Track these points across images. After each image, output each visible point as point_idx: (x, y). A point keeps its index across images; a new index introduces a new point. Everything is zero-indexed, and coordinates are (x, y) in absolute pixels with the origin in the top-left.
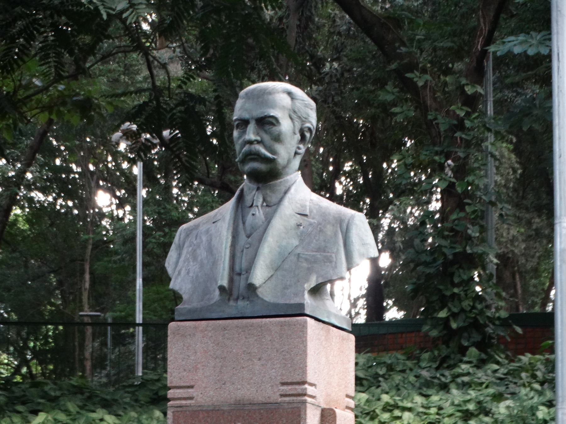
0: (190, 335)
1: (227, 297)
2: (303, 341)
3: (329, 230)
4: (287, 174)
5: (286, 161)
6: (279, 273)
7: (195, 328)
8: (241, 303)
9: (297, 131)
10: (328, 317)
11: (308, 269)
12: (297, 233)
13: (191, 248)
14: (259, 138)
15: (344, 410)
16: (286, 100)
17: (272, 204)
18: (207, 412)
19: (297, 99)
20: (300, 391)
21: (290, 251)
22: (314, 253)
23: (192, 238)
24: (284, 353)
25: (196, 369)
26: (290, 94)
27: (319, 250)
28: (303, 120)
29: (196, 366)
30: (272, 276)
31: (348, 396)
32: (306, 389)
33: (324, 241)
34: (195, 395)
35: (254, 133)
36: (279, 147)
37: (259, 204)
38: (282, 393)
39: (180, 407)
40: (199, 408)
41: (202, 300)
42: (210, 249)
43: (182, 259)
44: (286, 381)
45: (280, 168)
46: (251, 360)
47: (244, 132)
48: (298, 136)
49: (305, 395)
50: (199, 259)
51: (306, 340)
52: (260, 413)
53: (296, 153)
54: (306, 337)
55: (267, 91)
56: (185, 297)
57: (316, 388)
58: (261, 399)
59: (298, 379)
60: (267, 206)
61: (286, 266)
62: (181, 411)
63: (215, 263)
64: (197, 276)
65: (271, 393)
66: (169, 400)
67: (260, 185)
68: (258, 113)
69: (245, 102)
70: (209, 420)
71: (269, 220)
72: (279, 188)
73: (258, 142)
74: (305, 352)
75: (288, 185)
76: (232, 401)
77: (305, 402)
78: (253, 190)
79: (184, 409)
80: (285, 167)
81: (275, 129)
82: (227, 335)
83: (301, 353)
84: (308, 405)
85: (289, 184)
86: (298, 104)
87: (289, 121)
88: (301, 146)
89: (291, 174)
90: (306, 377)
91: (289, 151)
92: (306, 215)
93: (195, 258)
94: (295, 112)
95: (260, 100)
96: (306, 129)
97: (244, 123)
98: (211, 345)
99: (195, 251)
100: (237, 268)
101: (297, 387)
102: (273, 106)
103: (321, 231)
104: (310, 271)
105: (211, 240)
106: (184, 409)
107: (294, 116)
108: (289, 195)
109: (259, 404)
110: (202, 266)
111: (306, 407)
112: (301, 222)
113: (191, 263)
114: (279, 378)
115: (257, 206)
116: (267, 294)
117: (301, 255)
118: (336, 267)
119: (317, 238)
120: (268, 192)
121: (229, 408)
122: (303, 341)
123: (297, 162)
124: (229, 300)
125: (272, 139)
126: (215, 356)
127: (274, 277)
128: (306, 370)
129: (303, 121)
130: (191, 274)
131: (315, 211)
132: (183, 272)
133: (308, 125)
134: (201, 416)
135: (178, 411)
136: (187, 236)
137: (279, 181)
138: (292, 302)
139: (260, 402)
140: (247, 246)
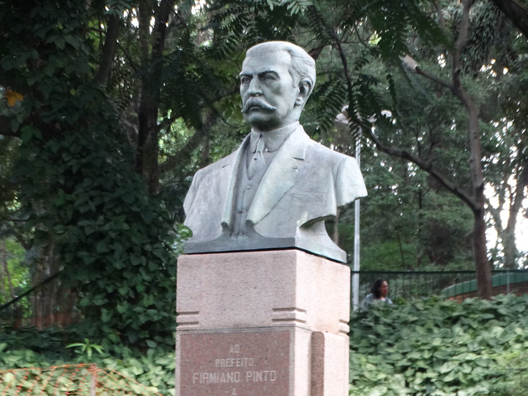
0: (196, 267)
1: (229, 233)
2: (292, 271)
3: (322, 172)
4: (288, 123)
6: (275, 211)
7: (201, 260)
8: (240, 238)
9: (296, 85)
10: (320, 250)
11: (301, 207)
13: (203, 190)
14: (260, 91)
15: (337, 334)
16: (286, 58)
17: (273, 150)
18: (210, 334)
19: (296, 56)
20: (289, 316)
22: (307, 193)
23: (205, 181)
24: (276, 282)
25: (201, 296)
26: (290, 51)
27: (311, 190)
28: (302, 75)
29: (201, 294)
30: (268, 213)
31: (341, 321)
32: (294, 314)
33: (317, 182)
34: (199, 320)
35: (256, 87)
36: (278, 99)
37: (261, 150)
38: (274, 318)
39: (187, 330)
40: (204, 332)
41: (208, 236)
42: (218, 191)
43: (196, 199)
44: (278, 307)
45: (280, 117)
46: (249, 289)
47: (247, 87)
48: (298, 89)
49: (294, 319)
50: (209, 199)
51: (295, 271)
52: (255, 336)
53: (296, 105)
54: (295, 268)
55: (269, 49)
56: (195, 233)
57: (306, 313)
58: (256, 323)
59: (287, 305)
60: (268, 151)
61: (282, 204)
62: (188, 335)
63: (220, 203)
64: (206, 215)
65: (265, 318)
66: (177, 325)
67: (263, 133)
68: (260, 69)
69: (250, 59)
70: (211, 342)
71: (268, 163)
73: (260, 95)
74: (294, 281)
75: (287, 133)
76: (231, 325)
77: (293, 326)
78: (257, 137)
79: (191, 332)
80: (284, 117)
81: (275, 83)
82: (227, 266)
83: (291, 282)
84: (296, 329)
85: (289, 132)
86: (297, 60)
87: (289, 76)
88: (301, 98)
89: (291, 123)
90: (295, 303)
91: (290, 103)
92: (302, 160)
93: (205, 198)
94: (294, 67)
95: (263, 57)
96: (306, 83)
97: (249, 77)
98: (215, 275)
99: (206, 192)
100: (239, 207)
101: (287, 312)
102: (274, 62)
103: (315, 173)
104: (302, 209)
105: (219, 182)
106: (191, 332)
107: (293, 71)
108: (287, 142)
109: (254, 328)
110: (210, 205)
111: (294, 330)
112: (297, 165)
113: (202, 203)
114: (271, 305)
115: (259, 152)
116: (264, 230)
117: (295, 195)
118: (326, 205)
119: (310, 180)
120: (269, 139)
121: (229, 332)
122: (292, 271)
123: (297, 113)
124: (231, 235)
125: (272, 92)
126: (217, 286)
127: (270, 215)
128: (295, 298)
130: (201, 213)
131: (310, 156)
132: (195, 211)
134: (205, 339)
135: (185, 335)
136: (201, 179)
137: (280, 129)
138: (285, 237)
139: (255, 326)
140: (249, 187)
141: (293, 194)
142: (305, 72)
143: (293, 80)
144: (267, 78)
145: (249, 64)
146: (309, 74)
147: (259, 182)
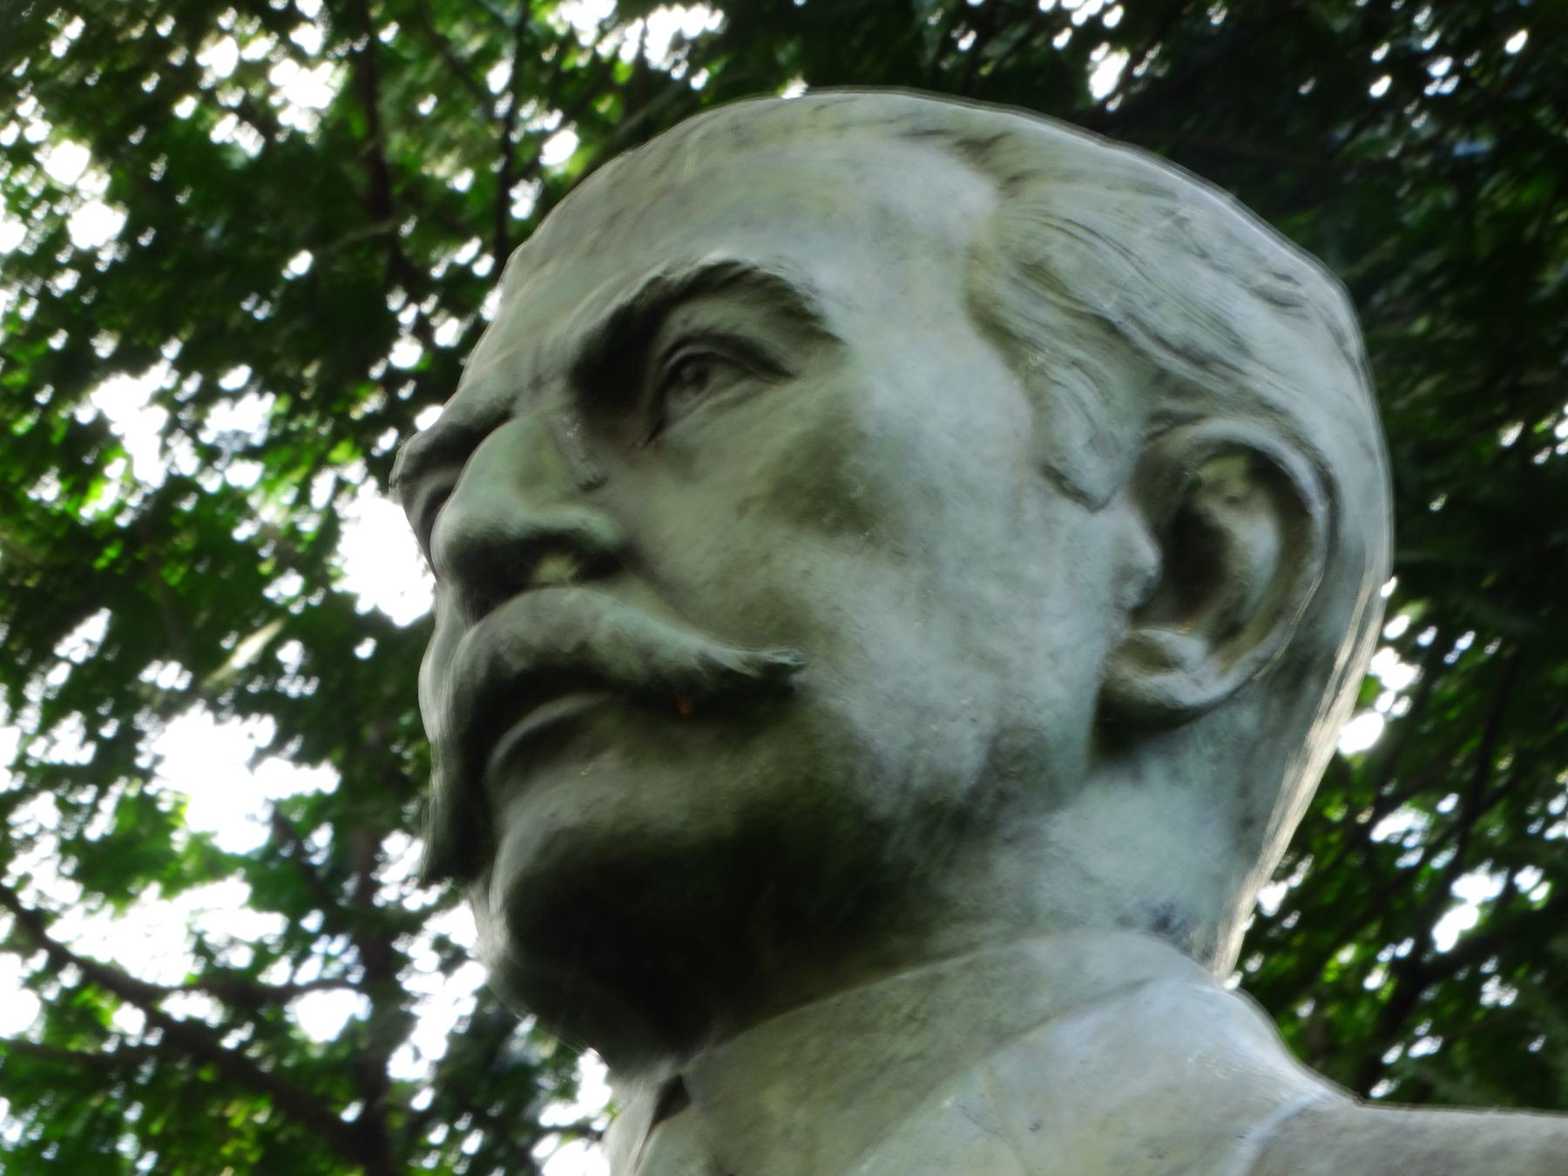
4: (1027, 920)
5: (961, 752)
26: (977, 149)
28: (1170, 378)
35: (529, 479)
48: (1126, 538)
72: (904, 1046)
88: (1184, 642)
94: (1036, 272)
96: (1233, 469)
129: (1161, 378)
142: (1208, 342)
143: (1039, 401)
144: (674, 380)
146: (1262, 383)
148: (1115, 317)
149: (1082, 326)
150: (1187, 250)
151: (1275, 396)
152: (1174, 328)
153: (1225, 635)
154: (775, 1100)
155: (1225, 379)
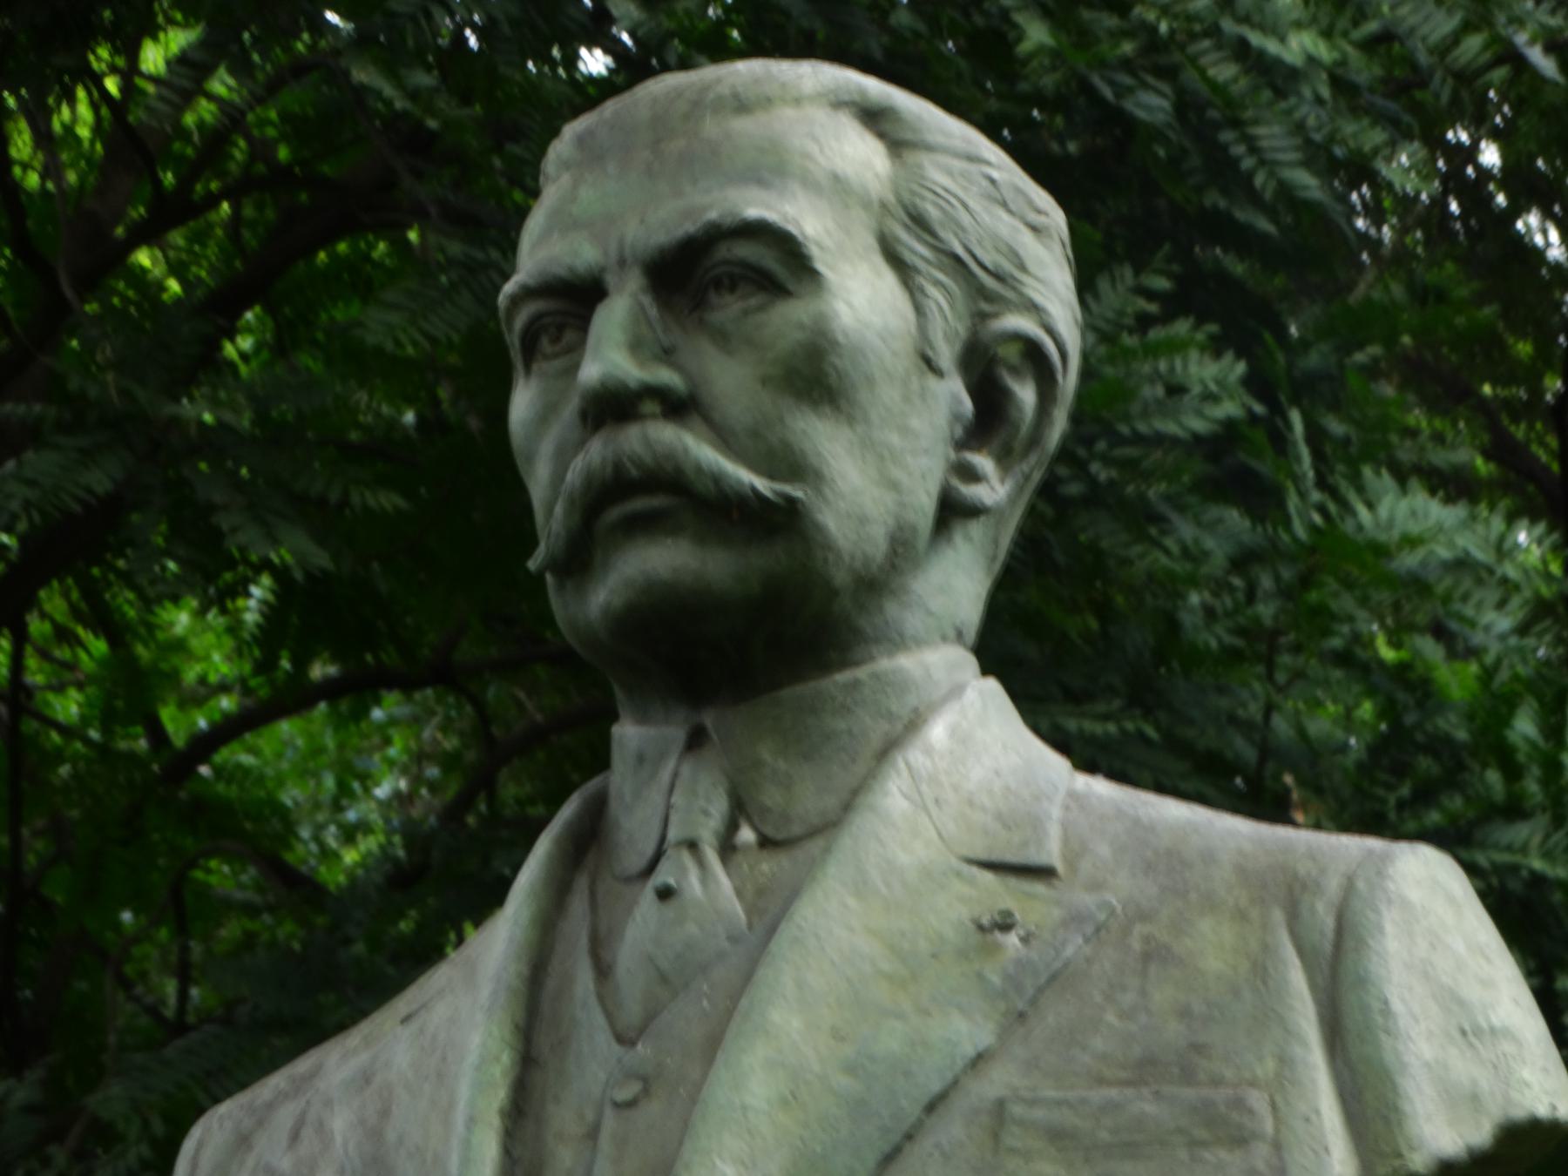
3: (1213, 946)
4: (898, 642)
5: (877, 545)
9: (946, 356)
12: (980, 976)
14: (666, 376)
17: (797, 829)
19: (929, 148)
21: (936, 1087)
22: (1113, 1093)
26: (873, 117)
27: (1146, 1070)
28: (985, 286)
35: (636, 346)
36: (825, 440)
37: (708, 831)
45: (841, 578)
53: (952, 511)
60: (765, 842)
67: (708, 719)
68: (662, 220)
71: (769, 913)
72: (841, 725)
78: (662, 756)
81: (786, 319)
88: (983, 462)
92: (1043, 873)
94: (919, 222)
103: (1154, 955)
105: (385, 1113)
107: (915, 249)
112: (1009, 903)
115: (693, 846)
119: (1128, 999)
120: (765, 752)
131: (1104, 850)
133: (1017, 322)
137: (842, 677)
140: (623, 1094)
141: (1000, 1106)
142: (1008, 267)
143: (919, 309)
144: (718, 284)
145: (579, 211)
147: (712, 1046)
148: (960, 251)
149: (945, 260)
150: (996, 201)
151: (1038, 298)
152: (988, 258)
153: (1005, 459)
154: (765, 752)
155: (1014, 289)
